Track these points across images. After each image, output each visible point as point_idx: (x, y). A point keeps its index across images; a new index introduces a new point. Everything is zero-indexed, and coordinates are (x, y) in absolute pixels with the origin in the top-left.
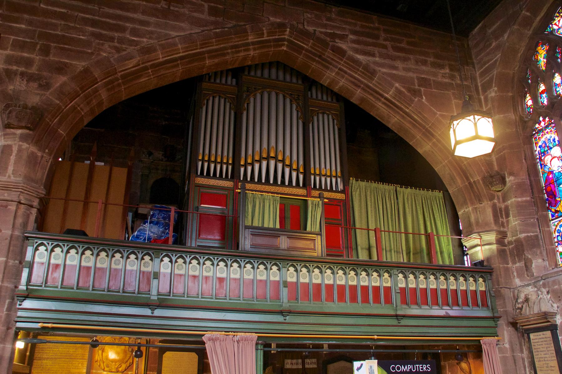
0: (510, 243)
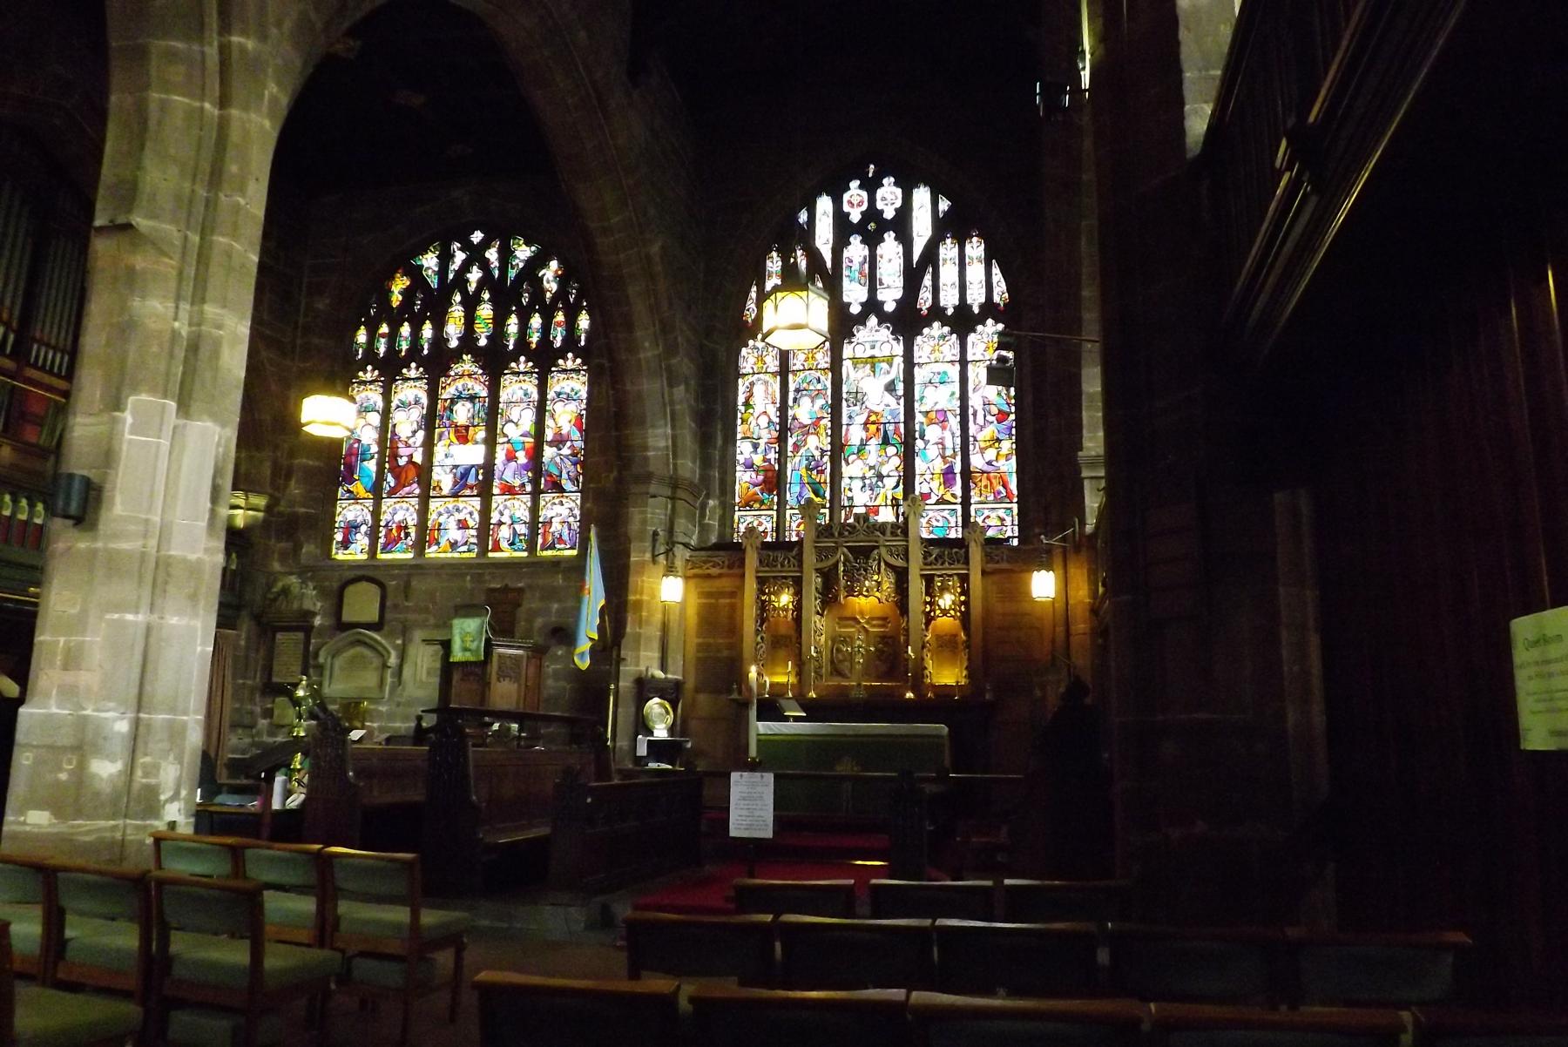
0: (281, 514)
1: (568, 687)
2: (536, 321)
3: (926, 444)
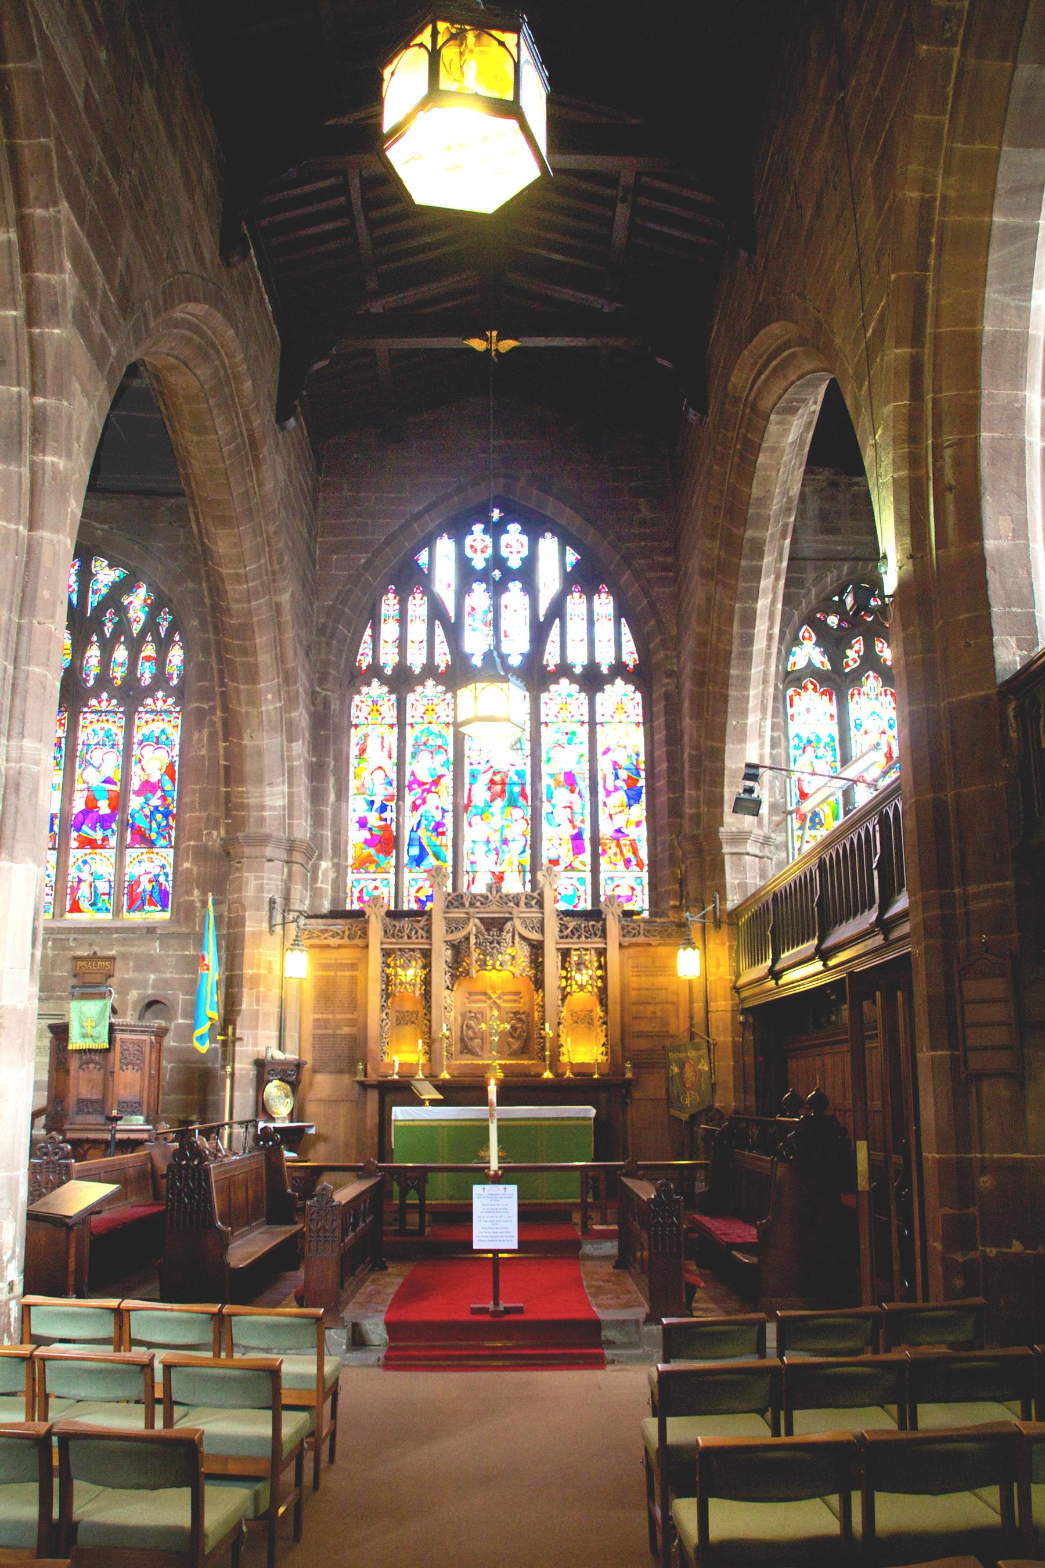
1: (169, 1066)
2: (121, 654)
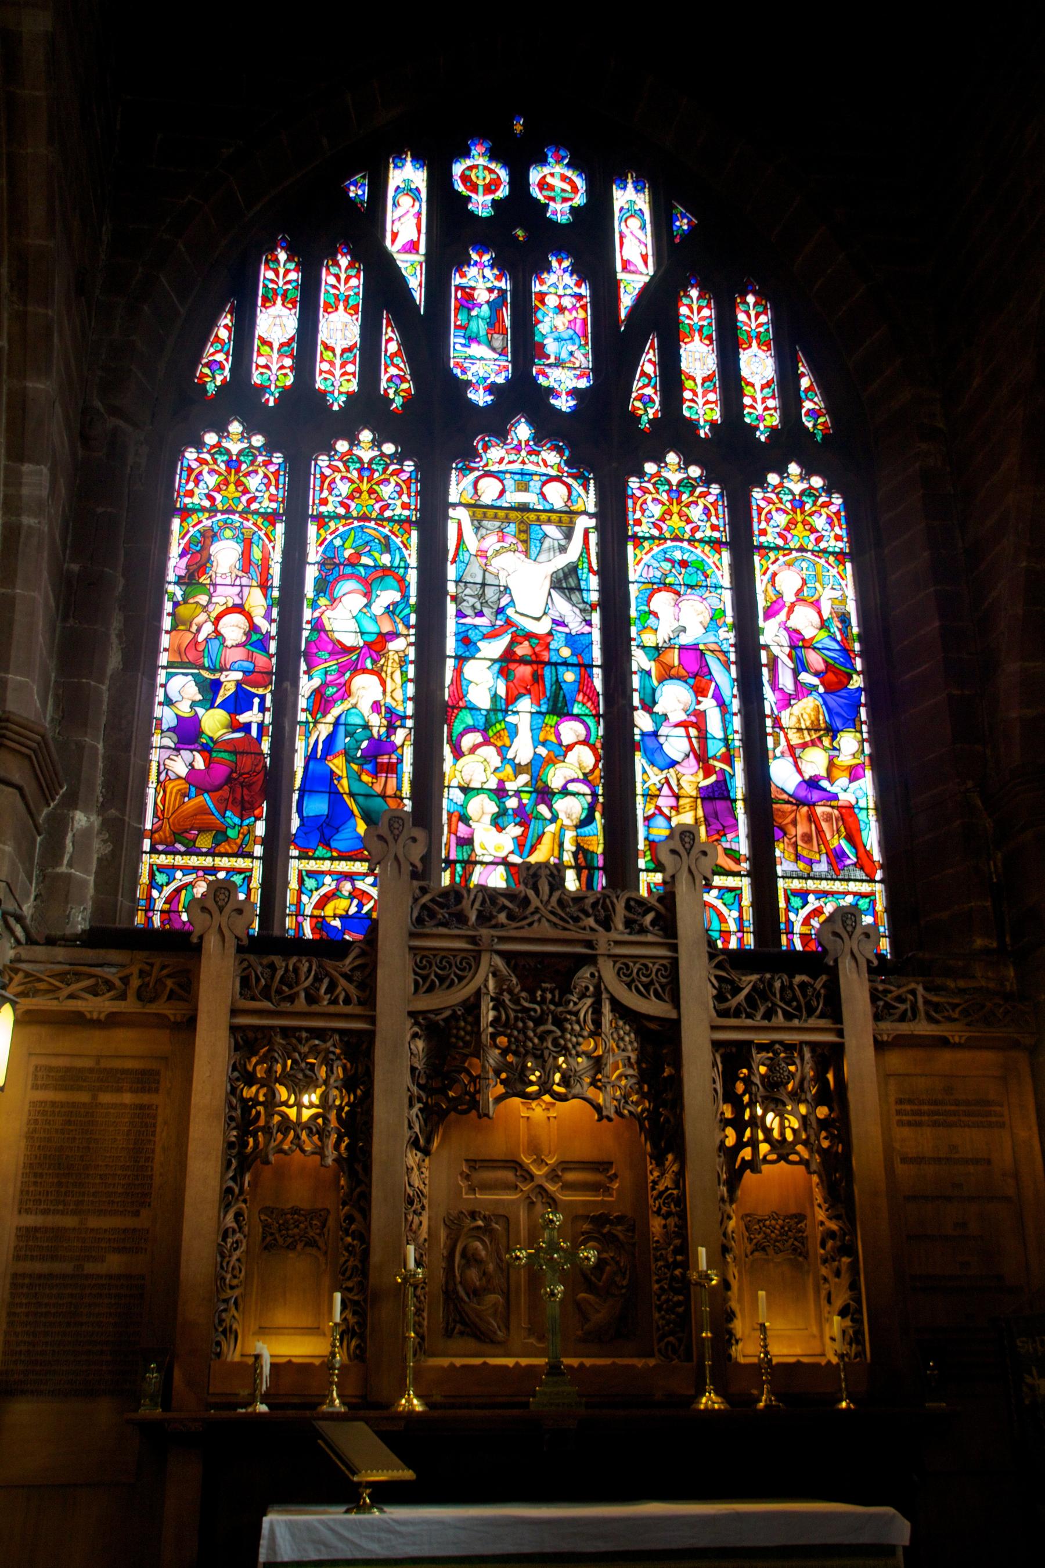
3: (658, 725)
